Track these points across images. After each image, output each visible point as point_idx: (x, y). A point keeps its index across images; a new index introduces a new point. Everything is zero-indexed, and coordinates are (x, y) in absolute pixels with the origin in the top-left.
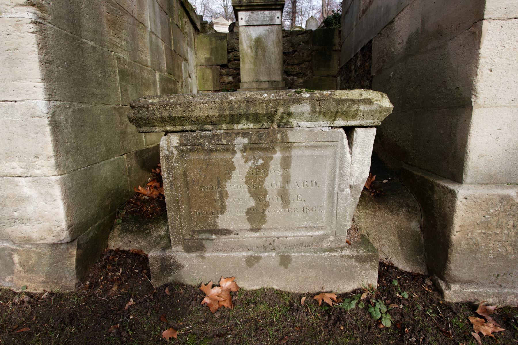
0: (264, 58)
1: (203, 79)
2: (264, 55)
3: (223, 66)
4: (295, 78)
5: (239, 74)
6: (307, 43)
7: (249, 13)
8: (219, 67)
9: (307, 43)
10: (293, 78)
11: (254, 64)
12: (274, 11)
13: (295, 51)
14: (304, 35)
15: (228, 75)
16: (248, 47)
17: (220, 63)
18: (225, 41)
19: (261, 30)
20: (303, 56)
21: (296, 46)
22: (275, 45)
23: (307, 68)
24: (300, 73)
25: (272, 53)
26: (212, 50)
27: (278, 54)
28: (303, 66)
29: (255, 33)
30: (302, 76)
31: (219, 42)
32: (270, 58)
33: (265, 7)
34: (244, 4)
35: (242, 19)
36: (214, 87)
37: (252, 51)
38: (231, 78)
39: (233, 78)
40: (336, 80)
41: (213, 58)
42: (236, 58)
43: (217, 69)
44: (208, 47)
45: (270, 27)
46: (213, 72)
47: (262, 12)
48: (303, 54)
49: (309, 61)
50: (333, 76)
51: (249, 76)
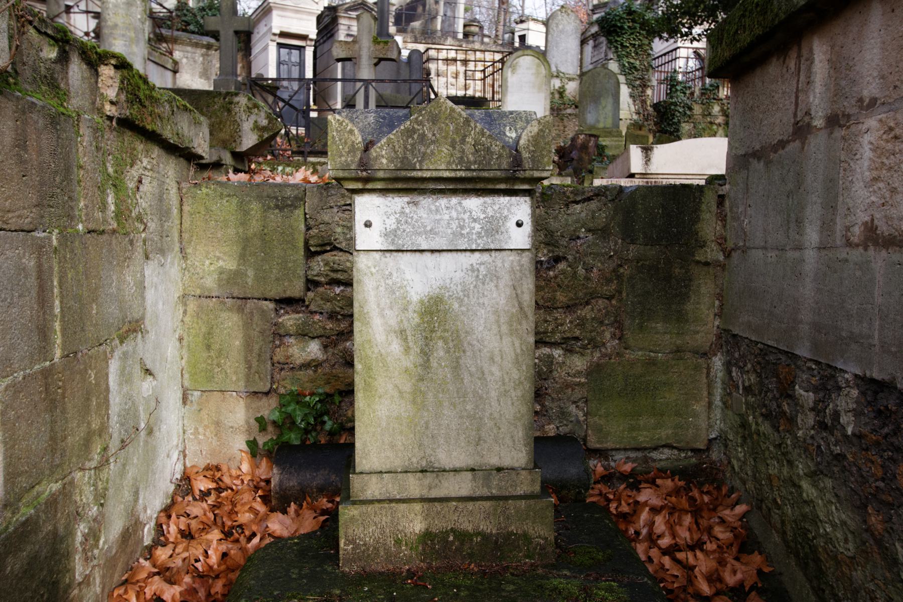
0: (458, 377)
1: (208, 347)
2: (456, 367)
3: (287, 302)
4: (557, 353)
5: (349, 334)
6: (603, 232)
7: (398, 202)
8: (271, 305)
9: (603, 232)
10: (551, 357)
11: (414, 402)
12: (504, 200)
13: (557, 260)
14: (593, 205)
15: (304, 335)
16: (389, 331)
17: (276, 291)
18: (299, 212)
19: (448, 271)
20: (588, 279)
21: (564, 242)
22: (505, 328)
23: (601, 323)
24: (577, 339)
25: (492, 359)
26: (245, 243)
27: (517, 362)
28: (586, 312)
29: (420, 278)
30: (584, 347)
31: (275, 217)
32: (482, 377)
33: (469, 186)
34: (381, 174)
35: (368, 225)
36: (248, 379)
37: (407, 350)
38: (314, 349)
39: (325, 347)
40: (709, 369)
41: (251, 273)
42: (339, 276)
43: (263, 312)
44: (231, 231)
45: (486, 257)
46: (247, 325)
47: (454, 200)
48: (589, 270)
49: (610, 298)
50: (696, 352)
51: (393, 446)
